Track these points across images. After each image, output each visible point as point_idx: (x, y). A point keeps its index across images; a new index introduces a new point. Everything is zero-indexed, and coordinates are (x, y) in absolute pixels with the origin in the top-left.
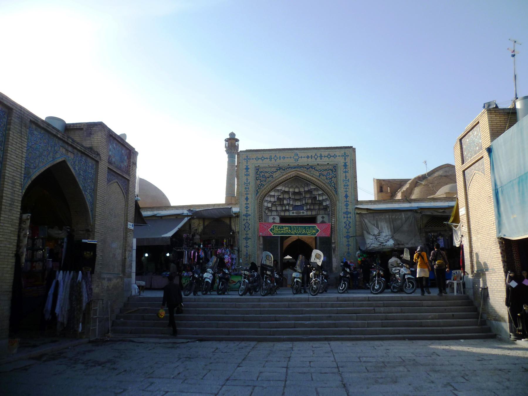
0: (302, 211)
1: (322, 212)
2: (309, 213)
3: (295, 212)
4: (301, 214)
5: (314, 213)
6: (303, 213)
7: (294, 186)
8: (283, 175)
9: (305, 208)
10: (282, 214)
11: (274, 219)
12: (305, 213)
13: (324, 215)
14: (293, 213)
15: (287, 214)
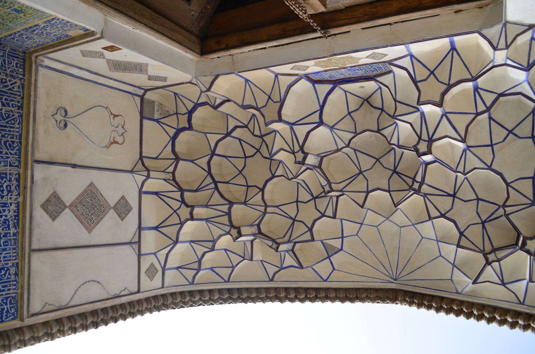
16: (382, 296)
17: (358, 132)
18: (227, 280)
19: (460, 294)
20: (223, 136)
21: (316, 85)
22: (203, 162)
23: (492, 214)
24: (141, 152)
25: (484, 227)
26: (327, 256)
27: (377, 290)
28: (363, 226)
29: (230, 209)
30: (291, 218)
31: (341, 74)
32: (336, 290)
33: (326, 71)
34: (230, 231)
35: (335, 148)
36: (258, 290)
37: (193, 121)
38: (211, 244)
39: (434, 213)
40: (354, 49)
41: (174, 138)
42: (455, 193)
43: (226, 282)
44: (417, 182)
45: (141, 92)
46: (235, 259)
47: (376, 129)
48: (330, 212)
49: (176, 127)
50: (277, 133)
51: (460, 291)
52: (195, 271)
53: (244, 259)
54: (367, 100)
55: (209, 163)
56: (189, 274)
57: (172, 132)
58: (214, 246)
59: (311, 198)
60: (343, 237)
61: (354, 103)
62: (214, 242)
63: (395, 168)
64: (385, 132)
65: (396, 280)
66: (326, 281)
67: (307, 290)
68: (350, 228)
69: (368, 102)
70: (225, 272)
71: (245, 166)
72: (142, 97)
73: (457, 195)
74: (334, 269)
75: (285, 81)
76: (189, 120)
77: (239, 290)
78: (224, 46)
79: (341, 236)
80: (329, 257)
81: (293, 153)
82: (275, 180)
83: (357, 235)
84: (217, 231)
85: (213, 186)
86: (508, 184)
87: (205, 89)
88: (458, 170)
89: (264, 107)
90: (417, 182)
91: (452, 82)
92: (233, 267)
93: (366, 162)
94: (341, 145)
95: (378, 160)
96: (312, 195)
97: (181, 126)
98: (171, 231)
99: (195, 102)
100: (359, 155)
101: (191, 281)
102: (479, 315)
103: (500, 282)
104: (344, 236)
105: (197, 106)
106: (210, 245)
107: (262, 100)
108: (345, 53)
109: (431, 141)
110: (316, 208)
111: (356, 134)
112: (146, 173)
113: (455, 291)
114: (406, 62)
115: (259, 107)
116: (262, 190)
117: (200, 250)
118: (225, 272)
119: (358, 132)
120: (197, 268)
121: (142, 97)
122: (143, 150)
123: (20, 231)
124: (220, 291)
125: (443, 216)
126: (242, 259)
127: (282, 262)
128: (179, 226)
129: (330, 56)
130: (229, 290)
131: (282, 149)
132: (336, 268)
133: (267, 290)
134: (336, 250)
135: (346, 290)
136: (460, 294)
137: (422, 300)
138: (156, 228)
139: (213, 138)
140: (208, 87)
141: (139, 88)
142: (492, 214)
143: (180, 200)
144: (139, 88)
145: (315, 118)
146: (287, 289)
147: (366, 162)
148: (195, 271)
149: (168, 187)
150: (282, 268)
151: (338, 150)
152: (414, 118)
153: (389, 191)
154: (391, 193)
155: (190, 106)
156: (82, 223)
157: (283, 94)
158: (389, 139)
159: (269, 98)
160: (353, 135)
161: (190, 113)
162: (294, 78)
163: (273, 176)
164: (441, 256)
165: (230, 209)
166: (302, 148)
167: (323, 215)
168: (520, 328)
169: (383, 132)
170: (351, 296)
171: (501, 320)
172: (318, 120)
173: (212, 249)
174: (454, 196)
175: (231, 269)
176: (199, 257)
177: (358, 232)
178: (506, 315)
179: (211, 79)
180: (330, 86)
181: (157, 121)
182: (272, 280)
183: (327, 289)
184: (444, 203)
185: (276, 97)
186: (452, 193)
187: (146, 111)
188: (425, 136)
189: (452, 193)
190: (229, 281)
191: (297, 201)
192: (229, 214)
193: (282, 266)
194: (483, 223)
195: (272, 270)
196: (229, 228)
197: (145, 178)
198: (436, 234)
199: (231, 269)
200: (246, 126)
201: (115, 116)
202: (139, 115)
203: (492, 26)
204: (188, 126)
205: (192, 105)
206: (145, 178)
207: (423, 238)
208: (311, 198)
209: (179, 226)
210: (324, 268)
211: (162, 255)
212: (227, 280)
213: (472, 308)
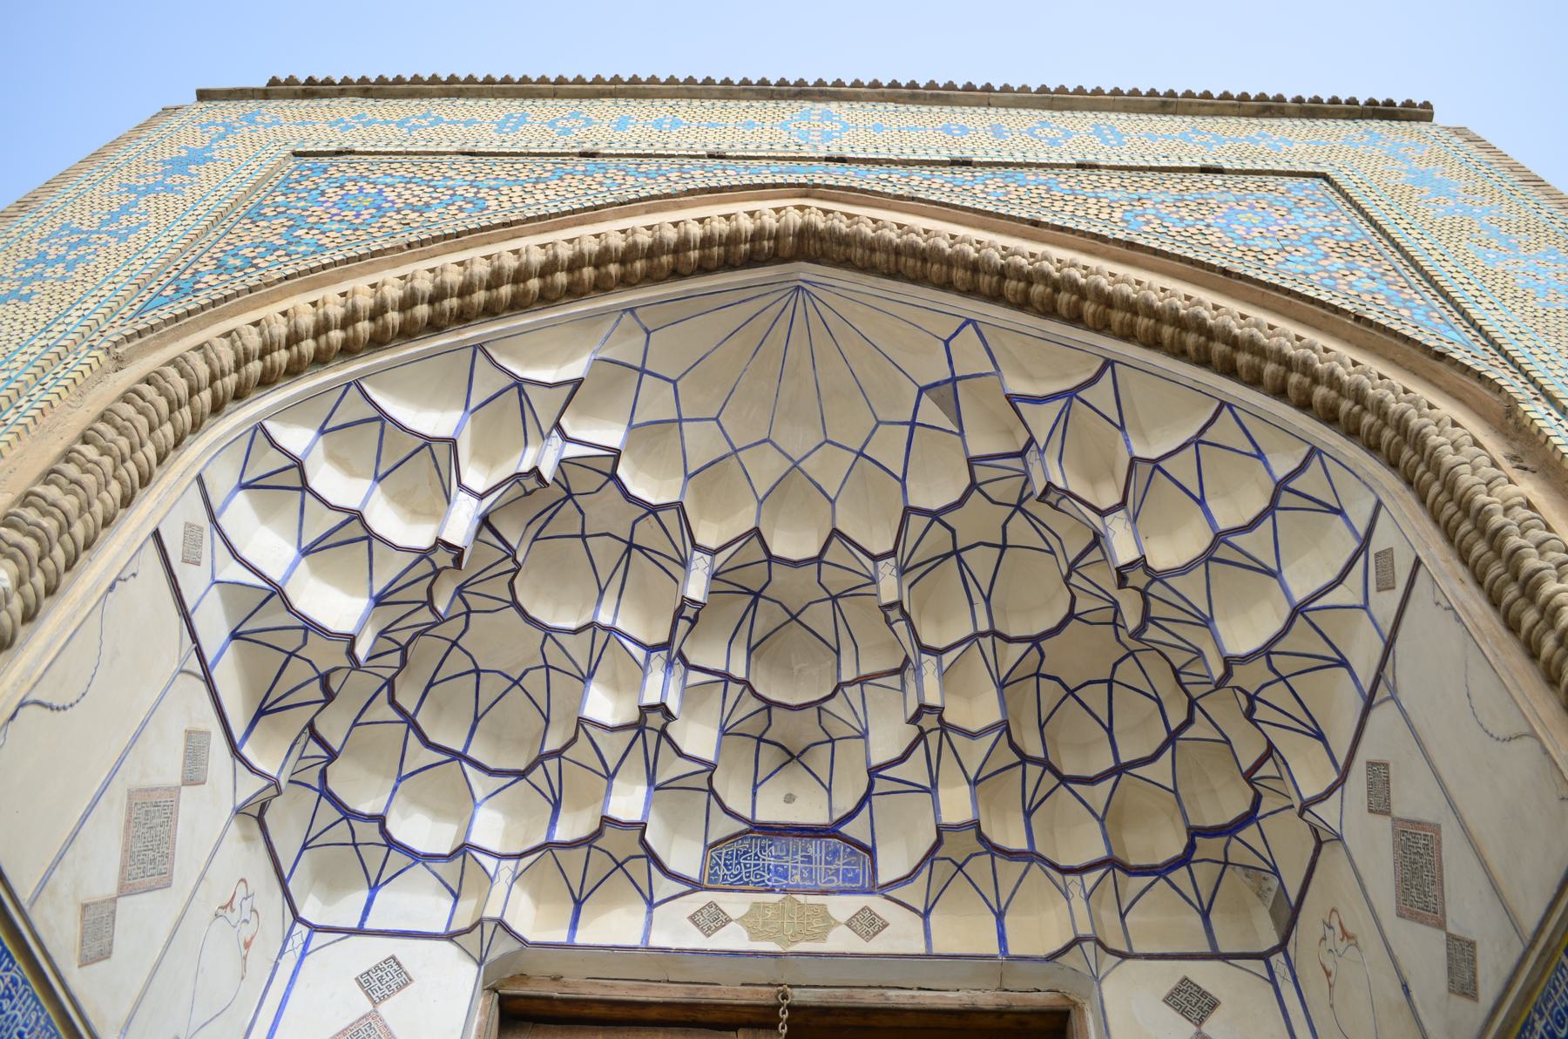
0: (843, 907)
1: (1161, 917)
2: (963, 930)
3: (735, 904)
4: (841, 941)
5: (1041, 925)
6: (869, 924)
7: (766, 468)
8: (624, 206)
9: (891, 865)
10: (534, 918)
11: (383, 981)
12: (901, 934)
13: (1206, 975)
14: (712, 920)
15: (615, 924)
16: (835, 248)
17: (814, 710)
18: (1226, 409)
19: (625, 311)
20: (1135, 771)
21: (869, 844)
22: (1200, 729)
23: (551, 517)
24: (1317, 851)
25: (568, 490)
26: (959, 384)
27: (846, 263)
28: (857, 448)
29: (1142, 628)
30: (1024, 512)
31: (809, 859)
32: (947, 285)
33: (825, 892)
34: (1151, 583)
35: (866, 687)
36: (1154, 343)
37: (1185, 840)
38: (1218, 554)
39: (669, 518)
40: (735, 959)
41: (1249, 818)
42: (628, 551)
43: (1230, 406)
44: (687, 618)
45: (1277, 960)
46: (1182, 468)
47: (774, 710)
48: (917, 523)
49: (1234, 841)
50: (972, 777)
51: (627, 317)
52: (1291, 485)
53: (1156, 463)
54: (793, 757)
55: (1189, 721)
56: (1310, 483)
57: (1249, 834)
58: (1214, 545)
59: (963, 555)
60: (913, 424)
61: (819, 759)
62: (1207, 557)
63: (755, 603)
64: (755, 704)
65: (798, 288)
66: (968, 321)
67: (1023, 304)
68: (888, 447)
69: (789, 753)
70: (1225, 430)
71: (1115, 665)
72: (1282, 947)
73: (625, 546)
74: (947, 343)
75: (914, 894)
76: (1191, 847)
77: (1204, 361)
78: (1008, 1017)
79: (917, 428)
80: (954, 380)
81: (944, 727)
82: (1037, 629)
83: (879, 423)
84: (1191, 587)
85: (1184, 678)
86: (515, 604)
87: (1085, 945)
88: (606, 634)
89: (1121, 660)
90: (687, 618)
91: (584, 850)
92: (1197, 441)
93: (820, 617)
94: (853, 692)
95: (794, 617)
96: (960, 561)
97: (1222, 840)
98: (1303, 638)
99: (1162, 881)
100: (832, 641)
101: (1317, 458)
102: (580, 268)
103: (526, 387)
104: (907, 428)
105: (1160, 871)
106: (1223, 552)
107: (980, 867)
108: (755, 954)
109: (639, 726)
110: (953, 531)
111: (818, 704)
112: (1307, 815)
113: (637, 312)
114: (664, 887)
115: (988, 856)
116: (1071, 615)
117: (1257, 544)
118: (1225, 430)
119: (814, 710)
120: (1284, 493)
121: (1282, 947)
122: (1310, 853)
123: (1530, 1007)
124: (1254, 381)
125: (653, 510)
126: (1162, 464)
127: (1065, 417)
128: (1274, 649)
129: (786, 954)
130: (1229, 370)
131: (973, 735)
132: (942, 345)
133: (1128, 335)
134: (934, 391)
135: (920, 280)
136: (625, 311)
137: (727, 252)
138: (1343, 663)
139: (1160, 771)
140: (1077, 948)
141: (1273, 981)
142: (551, 517)
143: (1257, 703)
144: (1273, 981)
145: (880, 786)
146: (1076, 319)
147: (820, 617)
148: (1291, 485)
149: (1280, 739)
150: (1070, 394)
151: (862, 680)
152: (671, 769)
153: (771, 558)
154: (764, 557)
155: (1180, 876)
156: (1441, 869)
157: (926, 871)
158: (747, 692)
159: (960, 868)
160: (826, 705)
161: (1185, 860)
162: (892, 893)
163: (1035, 641)
164: (674, 382)
165: (1142, 628)
166: (922, 736)
167: (935, 515)
168: (481, 280)
169: (759, 705)
170: (911, 262)
171: (524, 281)
172: (877, 780)
173: (1220, 537)
174: (631, 546)
175: (1205, 437)
176: (1269, 519)
177: (873, 431)
178: (514, 296)
179: (1065, 960)
180: (843, 829)
181: (1276, 872)
182: (1109, 363)
183: (972, 292)
184: (647, 533)
185: (942, 869)
186: (634, 551)
187: (1288, 916)
188: (652, 737)
189: (634, 551)
190: (1222, 404)
191: (1003, 547)
192: (1147, 618)
193: (1069, 403)
194: (570, 495)
195: (1101, 395)
196: (1150, 590)
197: (1313, 808)
198: (682, 438)
199: (1205, 437)
200: (1064, 780)
201: (1328, 974)
202: (1300, 921)
203: (503, 957)
204: (1197, 839)
205: (1172, 876)
206: (1313, 808)
207: (716, 419)
208: (963, 555)
209: (1274, 649)
210: (971, 357)
211: (1347, 594)
212: (1226, 409)
213: (597, 278)
